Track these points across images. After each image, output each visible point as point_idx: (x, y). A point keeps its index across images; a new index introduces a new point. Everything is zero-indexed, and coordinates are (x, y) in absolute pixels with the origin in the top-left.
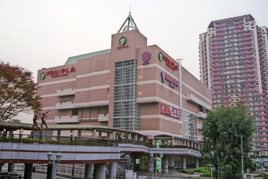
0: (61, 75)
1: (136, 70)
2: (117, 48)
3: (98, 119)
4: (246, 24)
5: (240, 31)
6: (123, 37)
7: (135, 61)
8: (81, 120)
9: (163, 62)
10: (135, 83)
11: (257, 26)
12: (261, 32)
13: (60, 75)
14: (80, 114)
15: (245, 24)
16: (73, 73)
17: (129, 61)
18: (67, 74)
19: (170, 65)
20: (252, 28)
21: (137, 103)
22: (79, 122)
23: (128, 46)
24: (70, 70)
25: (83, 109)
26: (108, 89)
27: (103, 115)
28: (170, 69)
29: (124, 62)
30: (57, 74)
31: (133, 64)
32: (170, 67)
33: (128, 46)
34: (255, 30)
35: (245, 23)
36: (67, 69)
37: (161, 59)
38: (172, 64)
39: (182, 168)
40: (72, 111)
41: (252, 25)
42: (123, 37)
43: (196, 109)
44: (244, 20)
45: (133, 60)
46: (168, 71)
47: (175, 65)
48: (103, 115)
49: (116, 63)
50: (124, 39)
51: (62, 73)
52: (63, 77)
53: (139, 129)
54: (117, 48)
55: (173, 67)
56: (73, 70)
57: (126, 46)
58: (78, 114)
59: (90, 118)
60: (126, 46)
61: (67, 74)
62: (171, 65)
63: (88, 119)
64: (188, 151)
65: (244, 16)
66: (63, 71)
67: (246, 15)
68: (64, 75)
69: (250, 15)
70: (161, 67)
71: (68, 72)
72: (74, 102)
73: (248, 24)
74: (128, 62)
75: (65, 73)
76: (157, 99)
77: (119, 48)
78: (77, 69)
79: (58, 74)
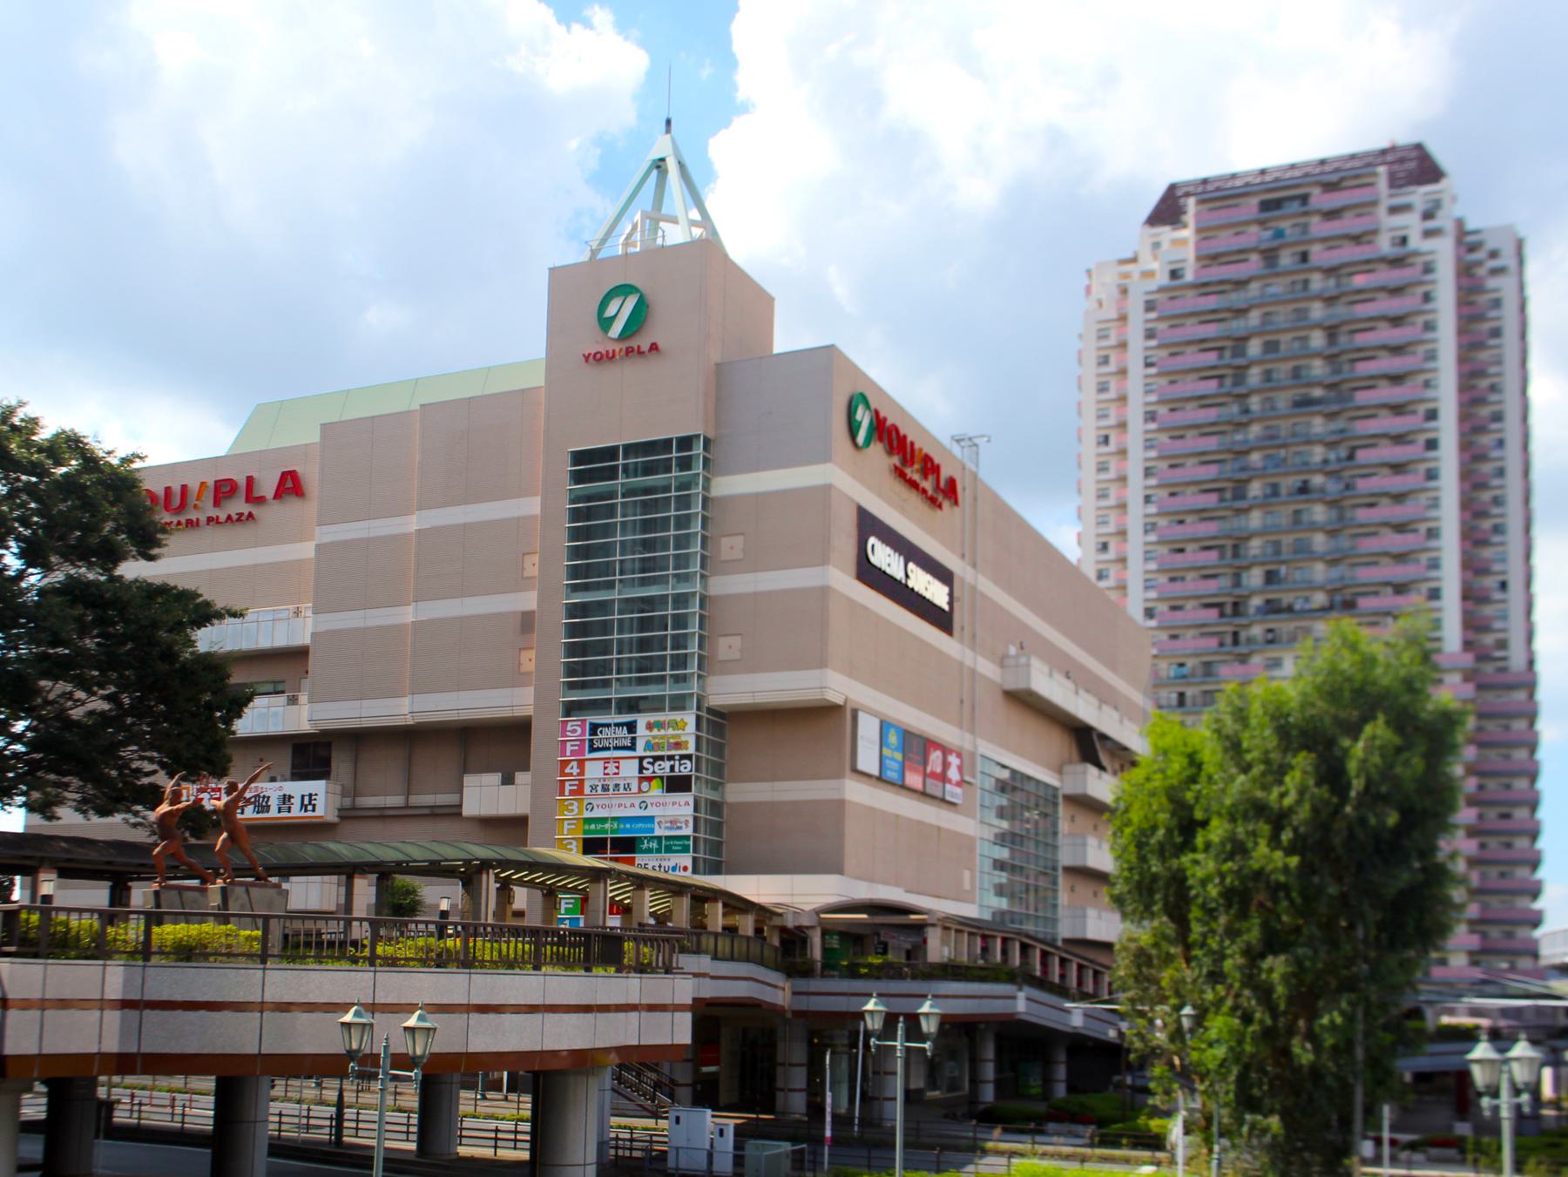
0: (210, 520)
1: (706, 500)
2: (587, 358)
3: (460, 806)
4: (1394, 210)
5: (1349, 253)
6: (623, 290)
7: (698, 449)
8: (354, 808)
9: (878, 457)
10: (698, 588)
11: (1460, 223)
12: (1479, 263)
13: (203, 519)
14: (341, 764)
15: (1382, 211)
16: (292, 506)
17: (666, 445)
18: (250, 515)
19: (913, 473)
20: (1428, 234)
21: (710, 711)
22: (336, 820)
23: (654, 347)
24: (267, 487)
25: (360, 739)
26: (527, 621)
27: (496, 778)
28: (914, 498)
29: (630, 449)
30: (183, 506)
31: (685, 464)
32: (913, 485)
33: (654, 347)
34: (1444, 252)
35: (1386, 202)
36: (250, 480)
37: (861, 438)
38: (930, 467)
39: (973, 1098)
40: (290, 751)
41: (1428, 215)
42: (623, 290)
43: (1058, 743)
44: (1382, 184)
45: (686, 443)
46: (903, 511)
47: (945, 473)
48: (496, 778)
49: (578, 457)
50: (631, 303)
51: (217, 503)
52: (220, 534)
53: (716, 869)
54: (587, 358)
55: (928, 485)
56: (290, 485)
57: (645, 348)
58: (333, 773)
59: (409, 794)
60: (645, 348)
61: (250, 515)
62: (916, 477)
63: (395, 800)
64: (1014, 998)
65: (1384, 152)
66: (223, 490)
67: (1393, 149)
68: (229, 518)
69: (1419, 147)
70: (861, 482)
71: (261, 500)
72: (303, 698)
73: (1405, 208)
74: (651, 454)
75: (238, 506)
76: (836, 686)
77: (599, 358)
78: (311, 476)
79: (193, 516)
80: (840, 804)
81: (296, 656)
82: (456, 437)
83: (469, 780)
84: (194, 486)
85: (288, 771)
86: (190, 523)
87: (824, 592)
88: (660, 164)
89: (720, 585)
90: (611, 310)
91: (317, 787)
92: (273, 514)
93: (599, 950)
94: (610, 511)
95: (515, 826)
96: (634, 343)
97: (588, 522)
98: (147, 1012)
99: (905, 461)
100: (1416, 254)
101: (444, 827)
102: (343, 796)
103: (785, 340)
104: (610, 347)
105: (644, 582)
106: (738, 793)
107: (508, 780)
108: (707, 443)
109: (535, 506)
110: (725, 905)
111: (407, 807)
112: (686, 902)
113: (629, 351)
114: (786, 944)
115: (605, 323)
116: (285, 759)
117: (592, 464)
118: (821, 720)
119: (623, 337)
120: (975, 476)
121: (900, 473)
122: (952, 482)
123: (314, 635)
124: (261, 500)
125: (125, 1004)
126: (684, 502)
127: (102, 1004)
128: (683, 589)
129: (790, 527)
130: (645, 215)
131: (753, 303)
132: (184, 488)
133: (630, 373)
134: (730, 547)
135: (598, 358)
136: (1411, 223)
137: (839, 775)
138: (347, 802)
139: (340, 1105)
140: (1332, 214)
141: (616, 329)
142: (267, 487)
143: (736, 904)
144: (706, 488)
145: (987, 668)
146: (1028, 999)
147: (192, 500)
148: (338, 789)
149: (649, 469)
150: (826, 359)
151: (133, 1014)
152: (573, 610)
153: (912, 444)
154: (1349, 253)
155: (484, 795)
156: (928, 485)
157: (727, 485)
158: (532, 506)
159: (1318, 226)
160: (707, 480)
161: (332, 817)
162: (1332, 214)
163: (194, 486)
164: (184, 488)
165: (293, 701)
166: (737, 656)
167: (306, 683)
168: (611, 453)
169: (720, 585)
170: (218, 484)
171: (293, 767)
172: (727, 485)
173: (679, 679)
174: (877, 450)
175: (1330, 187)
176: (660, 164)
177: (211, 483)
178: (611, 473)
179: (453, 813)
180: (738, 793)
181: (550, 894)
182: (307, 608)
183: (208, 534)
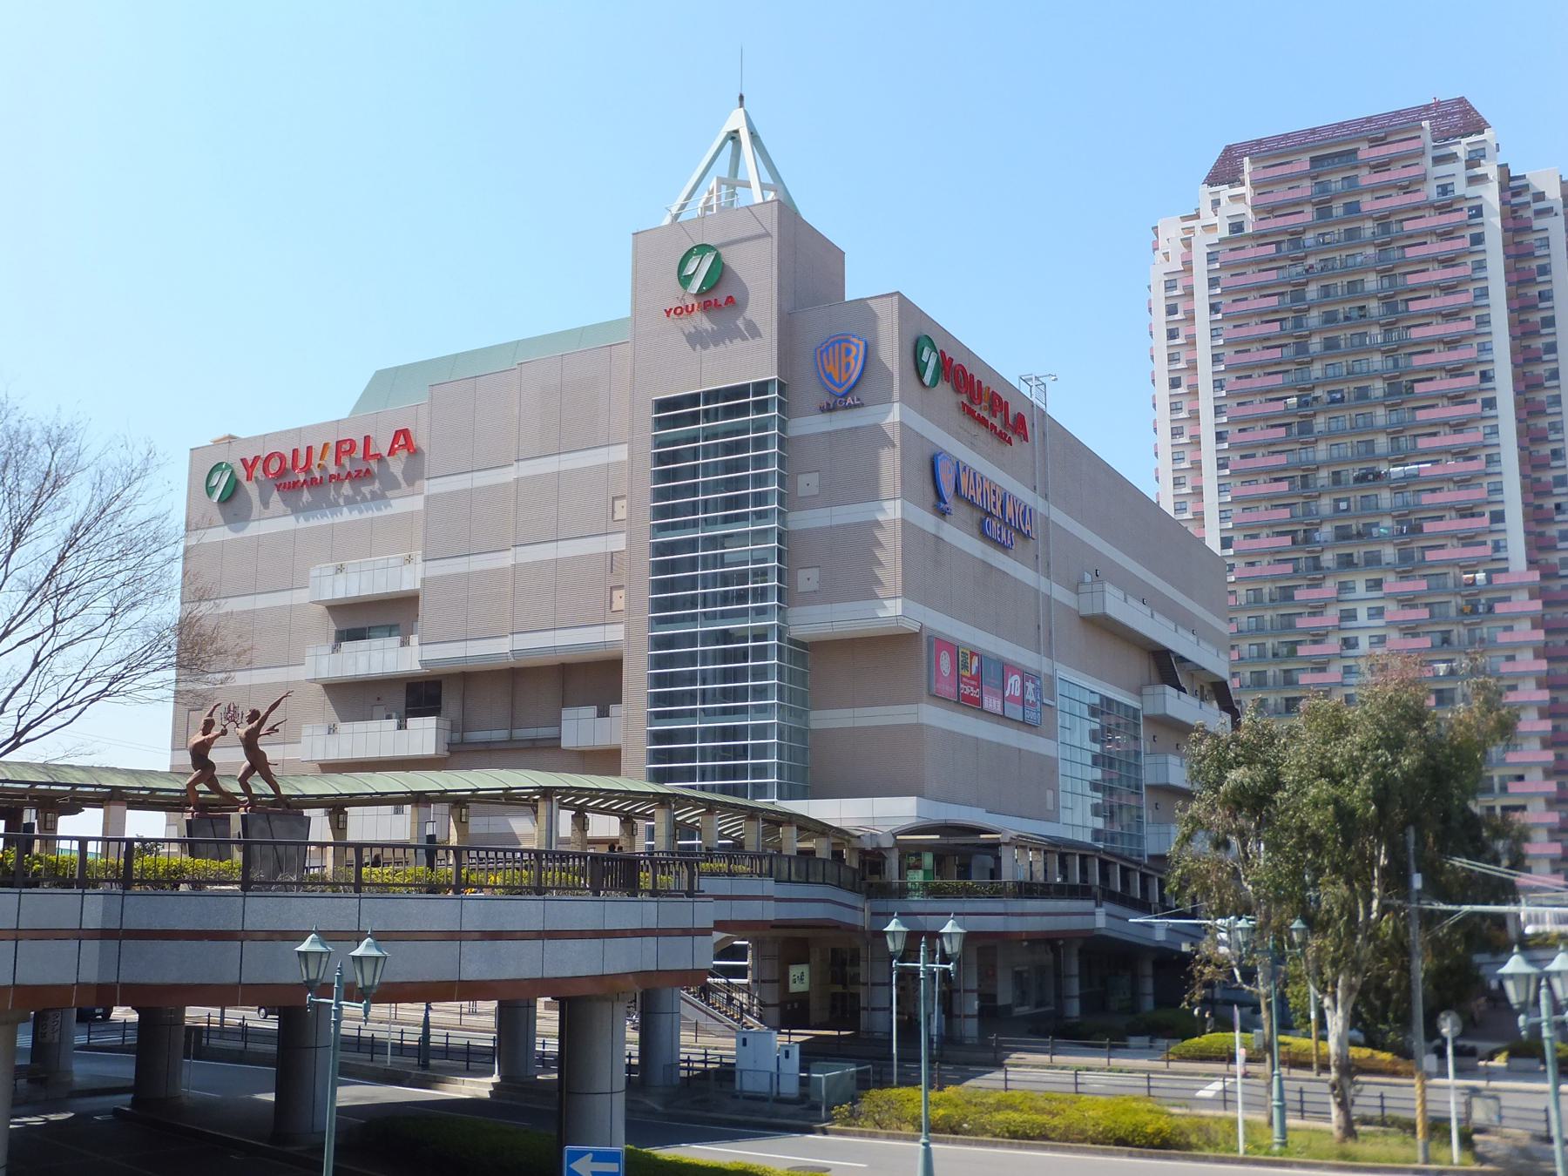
2: (668, 313)
4: (1438, 160)
5: (1399, 200)
8: (462, 743)
11: (1504, 168)
20: (1473, 180)
21: (792, 641)
23: (730, 300)
24: (382, 445)
25: (468, 680)
27: (593, 710)
28: (982, 434)
29: (711, 396)
32: (983, 421)
34: (1491, 195)
36: (367, 439)
37: (927, 379)
38: (997, 404)
41: (1472, 162)
42: (703, 249)
43: (1139, 667)
45: (761, 388)
46: (972, 446)
48: (593, 710)
49: (662, 405)
55: (996, 422)
57: (722, 301)
60: (722, 301)
61: (368, 471)
62: (985, 414)
63: (500, 735)
64: (1093, 914)
65: (1427, 108)
67: (1438, 104)
69: (1461, 101)
72: (414, 639)
73: (1453, 157)
82: (541, 386)
83: (567, 713)
96: (712, 298)
97: (669, 465)
99: (972, 399)
100: (1464, 198)
102: (452, 731)
104: (690, 301)
105: (727, 520)
107: (603, 713)
109: (623, 456)
111: (511, 740)
115: (685, 281)
117: (672, 410)
119: (700, 293)
120: (1043, 414)
122: (1020, 419)
123: (423, 580)
130: (721, 181)
136: (1457, 172)
138: (457, 737)
140: (1380, 166)
142: (382, 445)
145: (1060, 594)
146: (1107, 915)
148: (448, 724)
152: (659, 549)
153: (979, 382)
154: (1399, 200)
158: (620, 453)
159: (1366, 178)
162: (1380, 166)
165: (405, 643)
166: (816, 587)
170: (339, 444)
174: (944, 390)
175: (1376, 142)
177: (333, 445)
182: (418, 555)
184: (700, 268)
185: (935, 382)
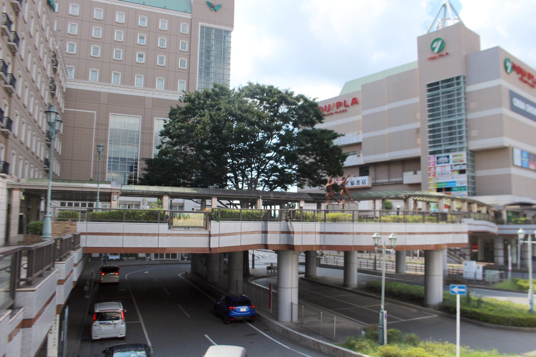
0: (336, 112)
1: (465, 93)
6: (437, 40)
7: (462, 79)
8: (375, 183)
9: (515, 75)
14: (371, 171)
16: (356, 106)
17: (452, 79)
19: (525, 79)
21: (471, 151)
23: (447, 54)
24: (349, 102)
25: (376, 165)
26: (418, 130)
28: (526, 86)
29: (443, 82)
30: (329, 110)
31: (458, 84)
32: (526, 82)
33: (447, 54)
36: (345, 101)
37: (509, 70)
42: (437, 40)
45: (458, 78)
48: (412, 173)
49: (429, 85)
50: (440, 43)
51: (337, 108)
53: (474, 195)
56: (355, 101)
59: (389, 178)
61: (345, 110)
63: (385, 180)
66: (339, 104)
68: (340, 111)
70: (510, 83)
71: (348, 106)
72: (361, 155)
74: (448, 82)
75: (342, 108)
76: (506, 141)
78: (360, 99)
79: (332, 112)
80: (509, 176)
81: (359, 144)
82: (395, 83)
83: (405, 174)
84: (331, 104)
85: (358, 174)
86: (331, 114)
87: (501, 115)
88: (444, 6)
89: (472, 116)
90: (434, 46)
91: (366, 178)
92: (351, 109)
93: (441, 217)
94: (439, 99)
95: (417, 186)
96: (441, 53)
97: (433, 102)
98: (326, 235)
101: (398, 187)
103: (484, 46)
105: (449, 117)
106: (479, 173)
108: (464, 77)
109: (419, 100)
110: (478, 205)
112: (466, 204)
113: (440, 56)
114: (497, 217)
115: (433, 49)
116: (357, 171)
117: (433, 87)
118: (503, 150)
119: (438, 52)
121: (521, 79)
123: (363, 139)
124: (348, 106)
125: (321, 233)
126: (459, 94)
127: (315, 233)
128: (460, 118)
129: (492, 97)
130: (442, 19)
131: (475, 38)
132: (329, 105)
133: (442, 61)
134: (472, 105)
135: (432, 59)
137: (508, 166)
138: (374, 182)
139: (375, 260)
141: (436, 50)
142: (349, 102)
143: (480, 205)
144: (465, 89)
147: (331, 108)
148: (371, 178)
149: (448, 86)
150: (497, 50)
151: (323, 235)
152: (430, 127)
155: (409, 177)
156: (530, 81)
157: (470, 88)
158: (417, 100)
160: (465, 88)
161: (370, 186)
163: (331, 104)
164: (329, 105)
165: (359, 156)
167: (361, 151)
168: (437, 83)
169: (472, 116)
170: (337, 103)
171: (360, 173)
172: (470, 88)
173: (461, 143)
174: (514, 74)
176: (444, 6)
177: (335, 103)
178: (438, 89)
179: (401, 183)
180: (479, 173)
181: (428, 203)
182: (361, 132)
183: (336, 116)
184: (437, 45)
185: (511, 71)
